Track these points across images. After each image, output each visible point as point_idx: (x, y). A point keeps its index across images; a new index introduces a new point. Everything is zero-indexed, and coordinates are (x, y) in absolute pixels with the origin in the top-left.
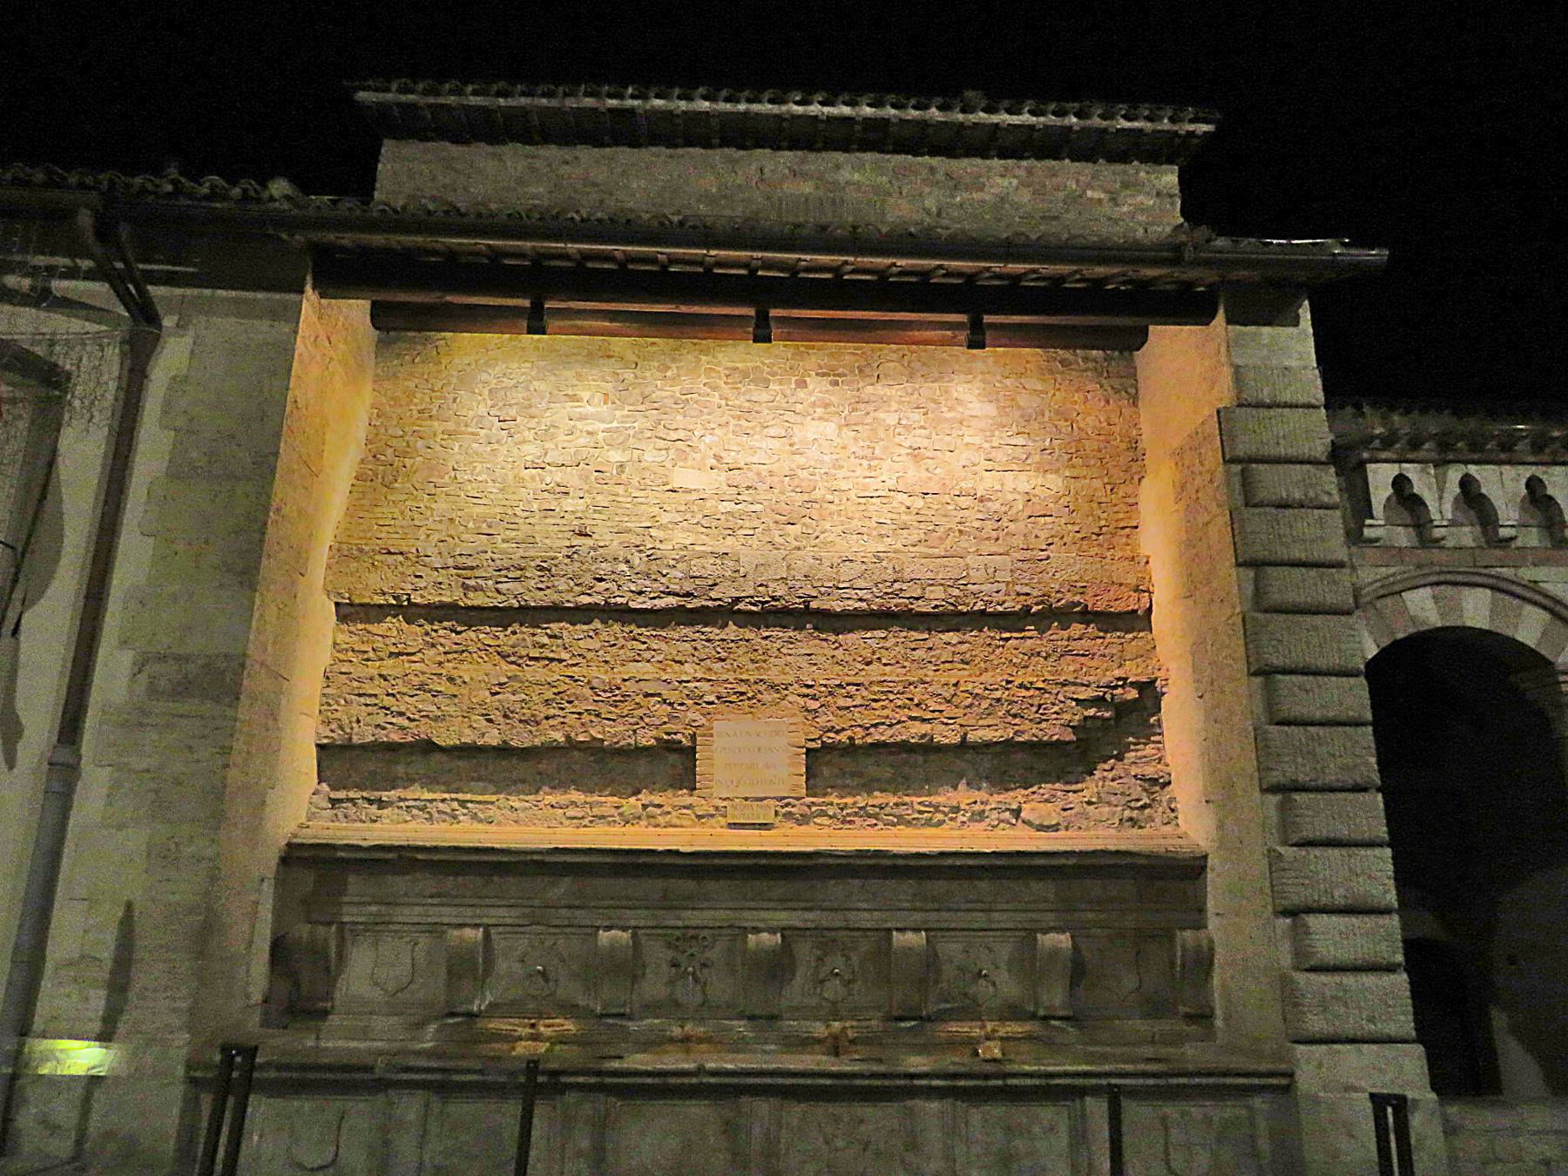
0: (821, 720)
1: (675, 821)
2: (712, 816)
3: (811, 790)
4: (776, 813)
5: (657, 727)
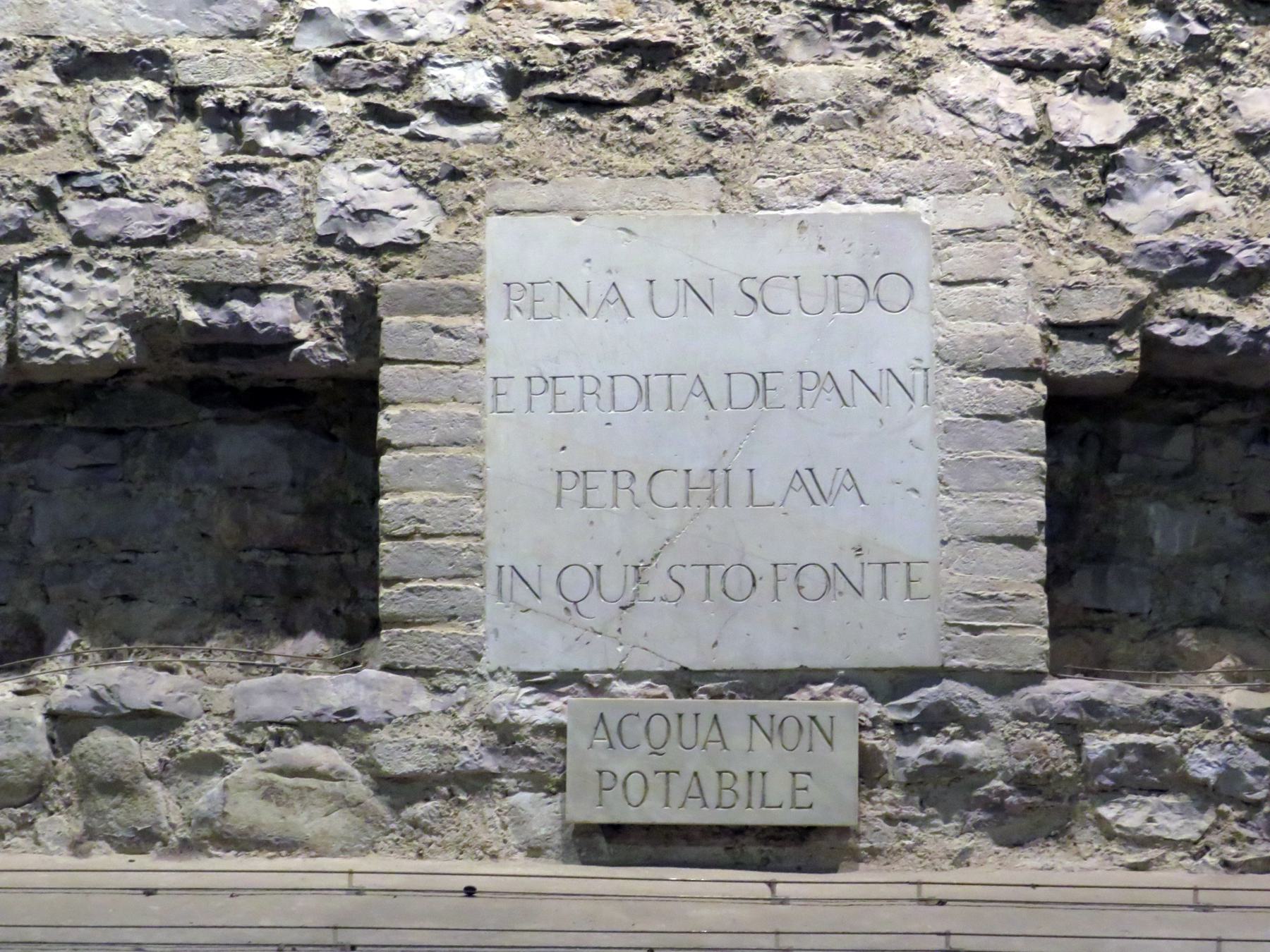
0: (1147, 212)
1: (250, 811)
2: (477, 782)
3: (1079, 633)
4: (870, 770)
5: (143, 251)
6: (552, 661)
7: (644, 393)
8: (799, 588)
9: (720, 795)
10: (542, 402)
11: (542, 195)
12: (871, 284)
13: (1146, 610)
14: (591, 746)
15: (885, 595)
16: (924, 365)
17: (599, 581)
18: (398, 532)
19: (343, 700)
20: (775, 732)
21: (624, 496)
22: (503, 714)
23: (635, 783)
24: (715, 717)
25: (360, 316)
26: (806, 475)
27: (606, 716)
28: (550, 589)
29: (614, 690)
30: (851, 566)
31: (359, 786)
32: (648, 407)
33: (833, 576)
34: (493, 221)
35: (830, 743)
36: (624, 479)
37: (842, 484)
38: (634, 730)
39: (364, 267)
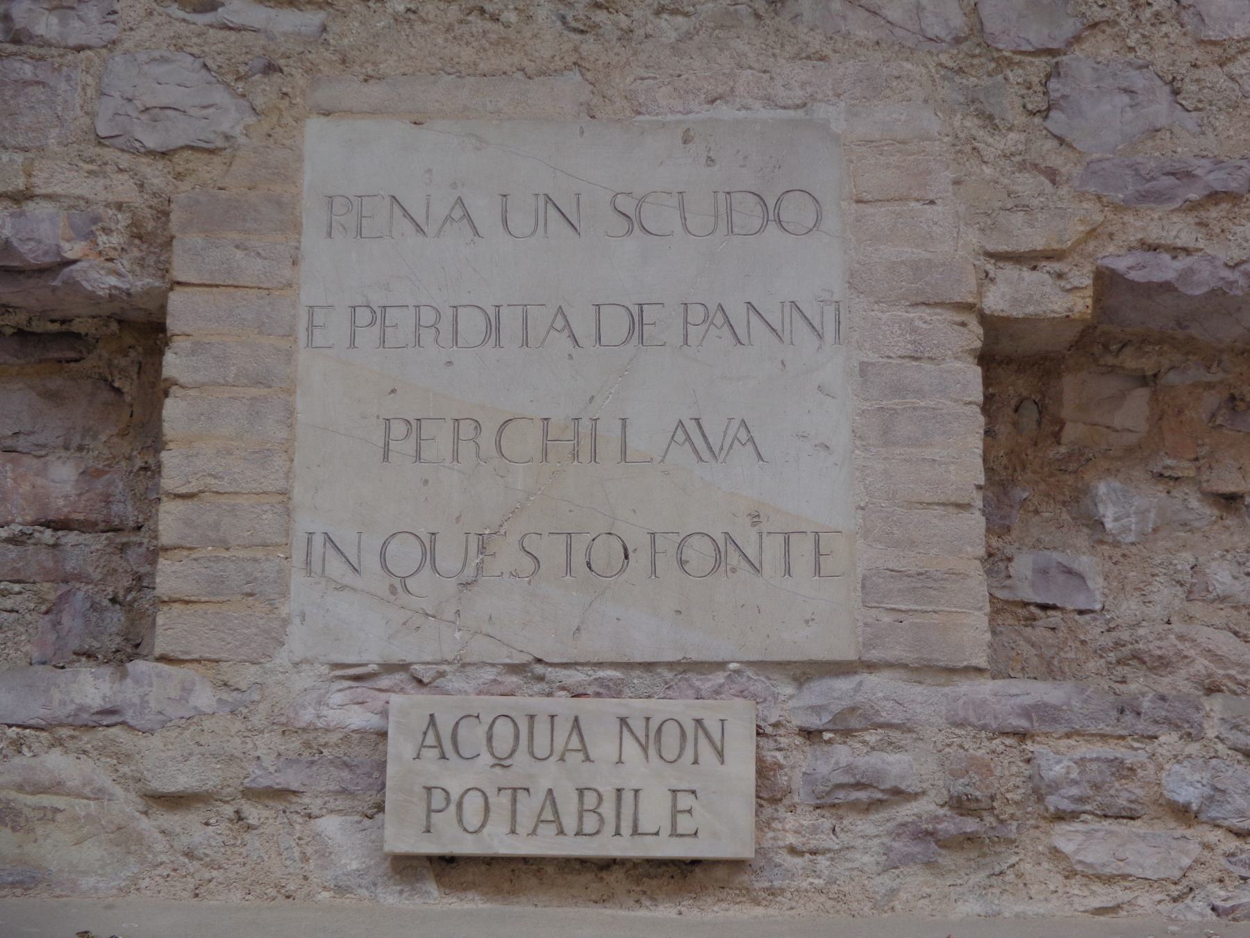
6: (371, 653)
7: (493, 327)
8: (682, 563)
9: (581, 818)
10: (369, 337)
11: (375, 92)
12: (771, 203)
13: (1098, 607)
14: (418, 757)
15: (788, 571)
16: (836, 298)
17: (433, 550)
18: (183, 490)
19: (104, 698)
20: (650, 741)
21: (467, 450)
22: (307, 716)
23: (473, 804)
24: (576, 719)
25: (151, 236)
26: (691, 426)
27: (438, 720)
28: (371, 562)
29: (450, 687)
30: (748, 539)
31: (125, 804)
32: (498, 343)
33: (724, 551)
34: (314, 125)
35: (720, 754)
36: (467, 429)
37: (736, 437)
38: (473, 735)
39: (156, 174)
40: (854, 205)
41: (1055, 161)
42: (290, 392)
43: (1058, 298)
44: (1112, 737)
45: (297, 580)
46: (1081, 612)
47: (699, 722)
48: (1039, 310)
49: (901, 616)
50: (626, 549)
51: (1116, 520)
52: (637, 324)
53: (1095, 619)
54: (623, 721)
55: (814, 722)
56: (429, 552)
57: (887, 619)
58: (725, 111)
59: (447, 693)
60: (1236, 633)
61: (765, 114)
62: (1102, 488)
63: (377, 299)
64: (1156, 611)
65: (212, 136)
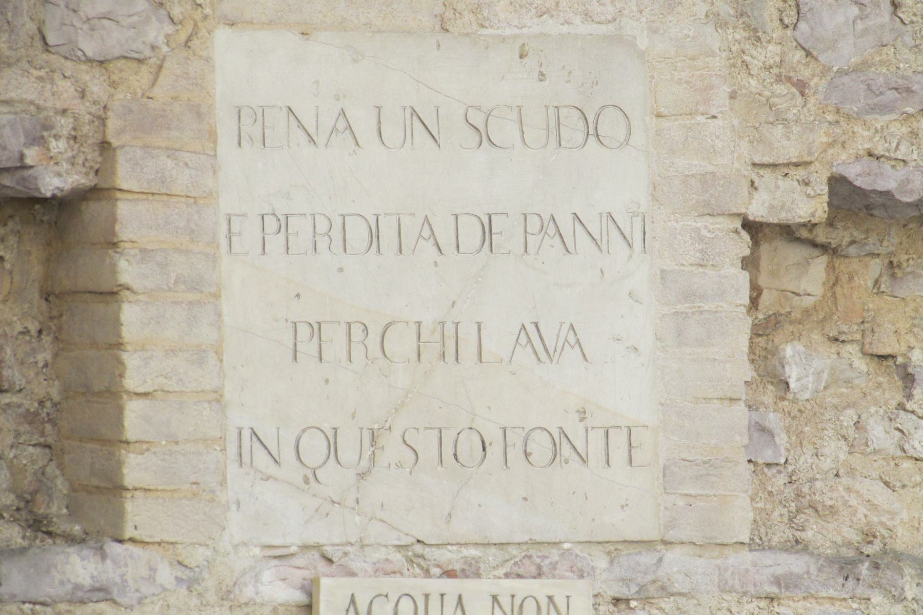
7: (374, 236)
8: (527, 454)
12: (591, 118)
13: (783, 461)
16: (642, 209)
24: (460, 597)
26: (531, 329)
34: (222, 35)
37: (566, 341)
40: (654, 119)
41: (805, 73)
42: (217, 296)
43: (808, 205)
44: (837, 599)
45: (232, 469)
46: (768, 465)
47: (550, 598)
48: (790, 216)
49: (691, 500)
50: (483, 442)
51: (798, 380)
52: (487, 232)
53: (779, 472)
54: (495, 598)
55: (623, 592)
56: (333, 448)
57: (681, 503)
58: (552, 26)
59: (353, 574)
60: (887, 484)
61: (584, 29)
62: (789, 351)
63: (282, 209)
64: (827, 464)
65: (141, 47)
